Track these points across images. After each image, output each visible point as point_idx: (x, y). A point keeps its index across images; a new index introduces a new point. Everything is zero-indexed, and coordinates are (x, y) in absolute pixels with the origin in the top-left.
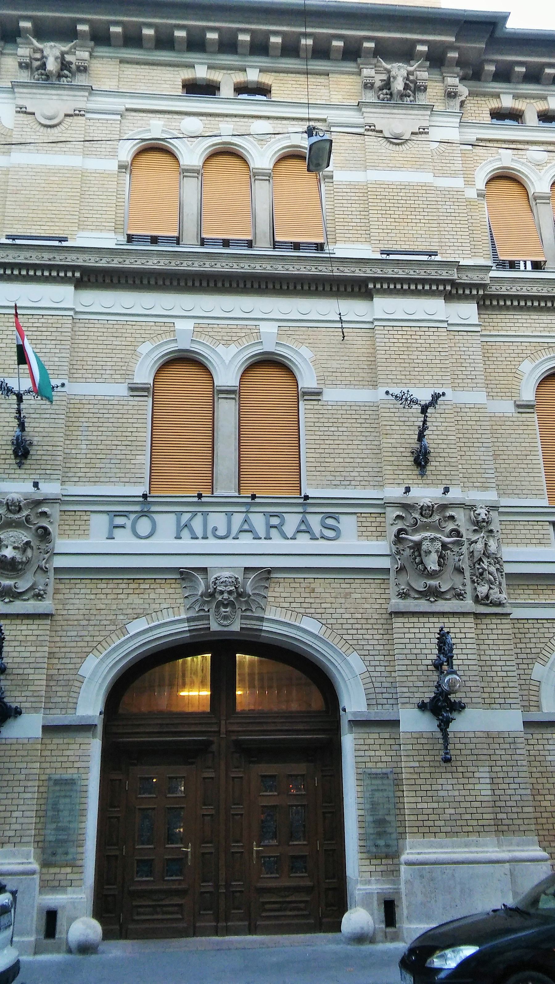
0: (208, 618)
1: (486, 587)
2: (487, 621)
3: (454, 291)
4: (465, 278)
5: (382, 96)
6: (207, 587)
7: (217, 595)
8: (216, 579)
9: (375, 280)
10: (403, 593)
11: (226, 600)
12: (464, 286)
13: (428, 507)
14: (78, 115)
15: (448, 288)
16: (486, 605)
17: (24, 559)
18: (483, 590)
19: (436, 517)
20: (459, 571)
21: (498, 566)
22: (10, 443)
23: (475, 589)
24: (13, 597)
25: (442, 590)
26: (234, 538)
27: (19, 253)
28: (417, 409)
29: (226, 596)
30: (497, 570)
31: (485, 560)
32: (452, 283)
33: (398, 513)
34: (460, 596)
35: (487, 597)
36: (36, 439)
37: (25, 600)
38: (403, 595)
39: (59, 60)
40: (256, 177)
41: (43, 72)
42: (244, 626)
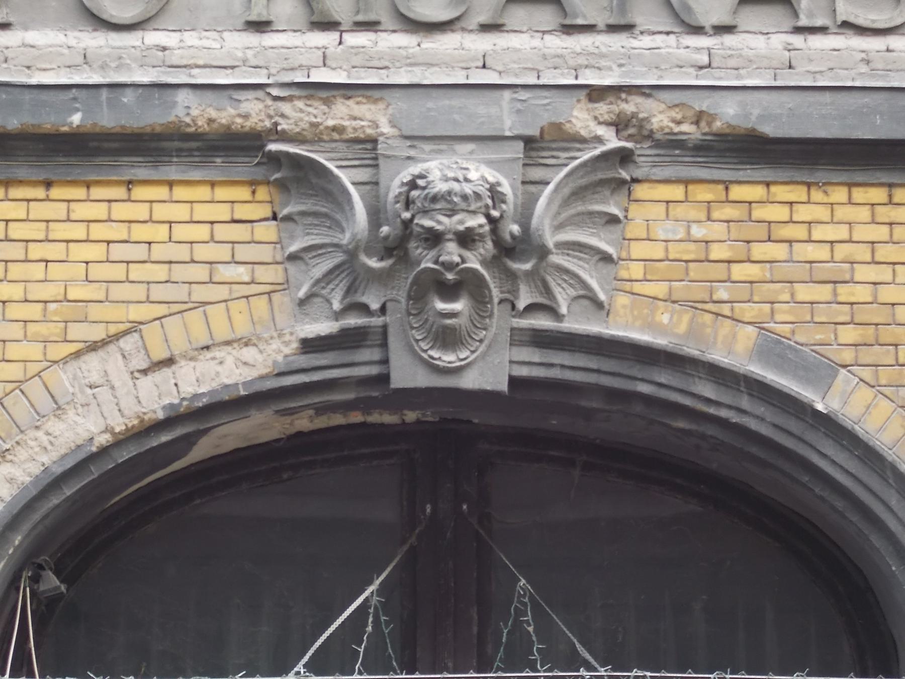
0: (383, 337)
6: (376, 215)
7: (415, 249)
8: (413, 185)
11: (450, 266)
26: (486, 28)
29: (452, 251)
42: (523, 372)
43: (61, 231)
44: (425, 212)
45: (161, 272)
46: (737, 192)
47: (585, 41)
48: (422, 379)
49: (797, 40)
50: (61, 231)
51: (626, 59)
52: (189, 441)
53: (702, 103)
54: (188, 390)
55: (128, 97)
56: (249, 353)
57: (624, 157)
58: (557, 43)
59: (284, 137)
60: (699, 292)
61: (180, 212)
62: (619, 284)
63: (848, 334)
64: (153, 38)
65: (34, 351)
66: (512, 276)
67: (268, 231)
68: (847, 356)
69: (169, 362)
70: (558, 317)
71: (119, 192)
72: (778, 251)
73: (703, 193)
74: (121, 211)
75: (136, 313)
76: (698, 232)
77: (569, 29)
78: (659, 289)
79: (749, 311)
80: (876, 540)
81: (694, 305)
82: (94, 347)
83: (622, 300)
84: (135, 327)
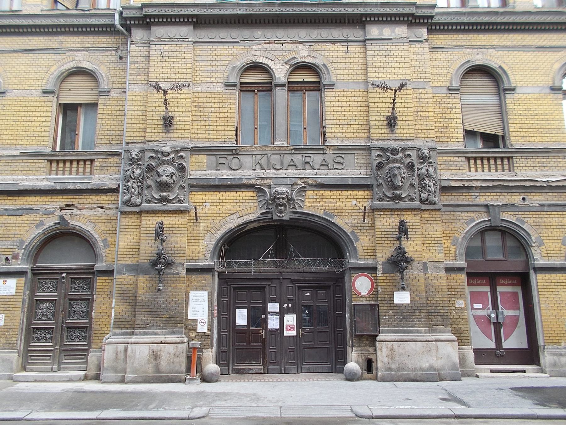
1: (427, 194)
2: (426, 213)
3: (413, 21)
4: (419, 12)
6: (271, 196)
8: (276, 191)
9: (366, 15)
10: (381, 198)
11: (281, 202)
12: (420, 17)
13: (396, 149)
15: (410, 19)
16: (427, 204)
17: (172, 181)
18: (424, 196)
19: (401, 155)
20: (412, 185)
21: (434, 182)
22: (162, 118)
23: (420, 195)
24: (168, 202)
25: (403, 196)
26: (285, 169)
27: (162, 8)
28: (390, 93)
30: (433, 184)
31: (426, 179)
33: (379, 153)
34: (412, 200)
35: (427, 200)
36: (176, 115)
37: (173, 203)
38: (381, 200)
42: (292, 217)
43: (227, 198)
44: (277, 195)
45: (241, 204)
46: (320, 192)
47: (299, 171)
48: (278, 218)
49: (329, 170)
50: (227, 198)
51: (305, 173)
52: (245, 227)
53: (316, 179)
54: (245, 220)
55: (236, 180)
56: (253, 215)
57: (305, 187)
58: (295, 171)
59: (258, 185)
60: (316, 205)
61: (244, 195)
62: (305, 205)
63: (336, 211)
64: (240, 171)
65: (224, 215)
66: (290, 203)
67: (256, 198)
68: (336, 214)
69: (243, 216)
70: (296, 209)
71: (235, 193)
72: (327, 200)
73: (316, 192)
74: (235, 195)
75: (238, 209)
76: (315, 197)
77: (297, 169)
78: (310, 205)
79: (322, 208)
80: (340, 239)
81: (315, 207)
82: (232, 214)
83: (305, 207)
84: (238, 212)
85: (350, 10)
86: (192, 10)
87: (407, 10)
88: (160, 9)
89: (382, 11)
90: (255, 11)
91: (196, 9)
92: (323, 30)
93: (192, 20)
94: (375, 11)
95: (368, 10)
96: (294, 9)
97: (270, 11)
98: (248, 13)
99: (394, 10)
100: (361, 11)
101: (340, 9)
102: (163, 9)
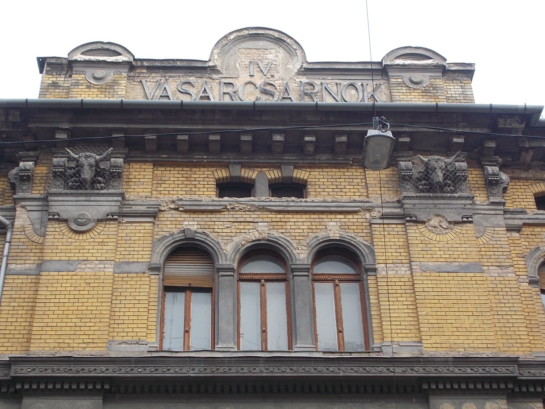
3: (517, 390)
4: (526, 374)
5: (421, 187)
9: (429, 380)
14: (110, 220)
15: (510, 386)
27: (47, 366)
32: (514, 379)
39: (94, 168)
40: (295, 274)
41: (77, 179)
85: (399, 371)
86: (104, 369)
87: (503, 371)
88: (42, 367)
89: (456, 372)
90: (221, 372)
91: (111, 367)
92: (350, 404)
93: (102, 387)
94: (444, 372)
95: (431, 371)
96: (295, 368)
97: (250, 372)
98: (209, 375)
99: (479, 372)
100: (419, 371)
101: (379, 369)
102: (49, 367)
